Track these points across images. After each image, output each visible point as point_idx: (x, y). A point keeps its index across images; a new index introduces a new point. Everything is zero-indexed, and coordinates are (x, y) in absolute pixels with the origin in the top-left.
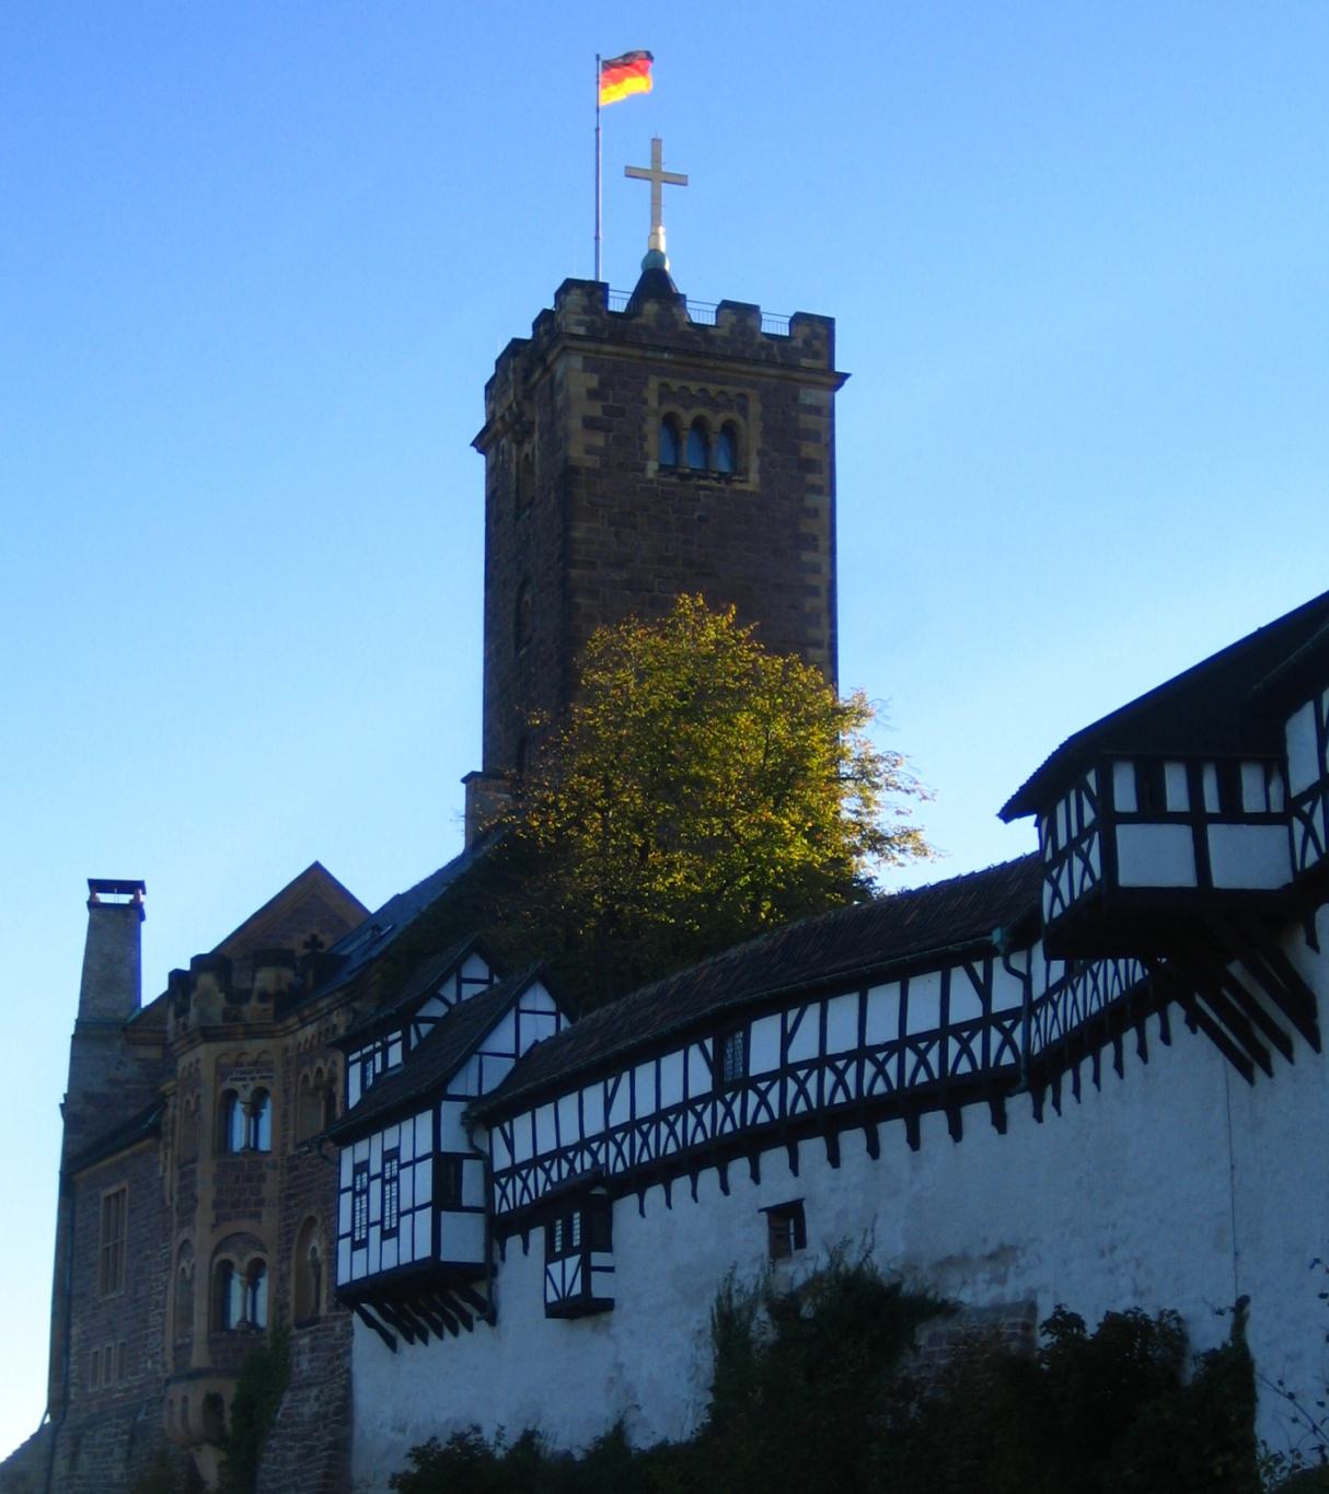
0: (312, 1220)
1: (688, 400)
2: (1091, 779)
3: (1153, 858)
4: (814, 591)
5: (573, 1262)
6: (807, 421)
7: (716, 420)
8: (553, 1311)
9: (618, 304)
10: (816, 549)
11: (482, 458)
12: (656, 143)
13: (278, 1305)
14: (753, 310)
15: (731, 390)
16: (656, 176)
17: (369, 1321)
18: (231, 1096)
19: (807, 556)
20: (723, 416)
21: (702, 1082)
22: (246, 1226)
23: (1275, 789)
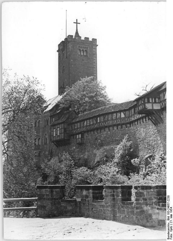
0: (46, 134)
1: (82, 47)
2: (143, 99)
3: (149, 106)
4: (95, 68)
5: (80, 139)
6: (94, 50)
7: (84, 50)
8: (77, 144)
9: (74, 37)
10: (95, 63)
11: (58, 53)
12: (77, 20)
13: (42, 142)
14: (88, 38)
15: (86, 47)
16: (77, 23)
17: (55, 145)
18: (36, 121)
19: (94, 64)
20: (85, 49)
21: (95, 122)
22: (38, 134)
23: (159, 100)
